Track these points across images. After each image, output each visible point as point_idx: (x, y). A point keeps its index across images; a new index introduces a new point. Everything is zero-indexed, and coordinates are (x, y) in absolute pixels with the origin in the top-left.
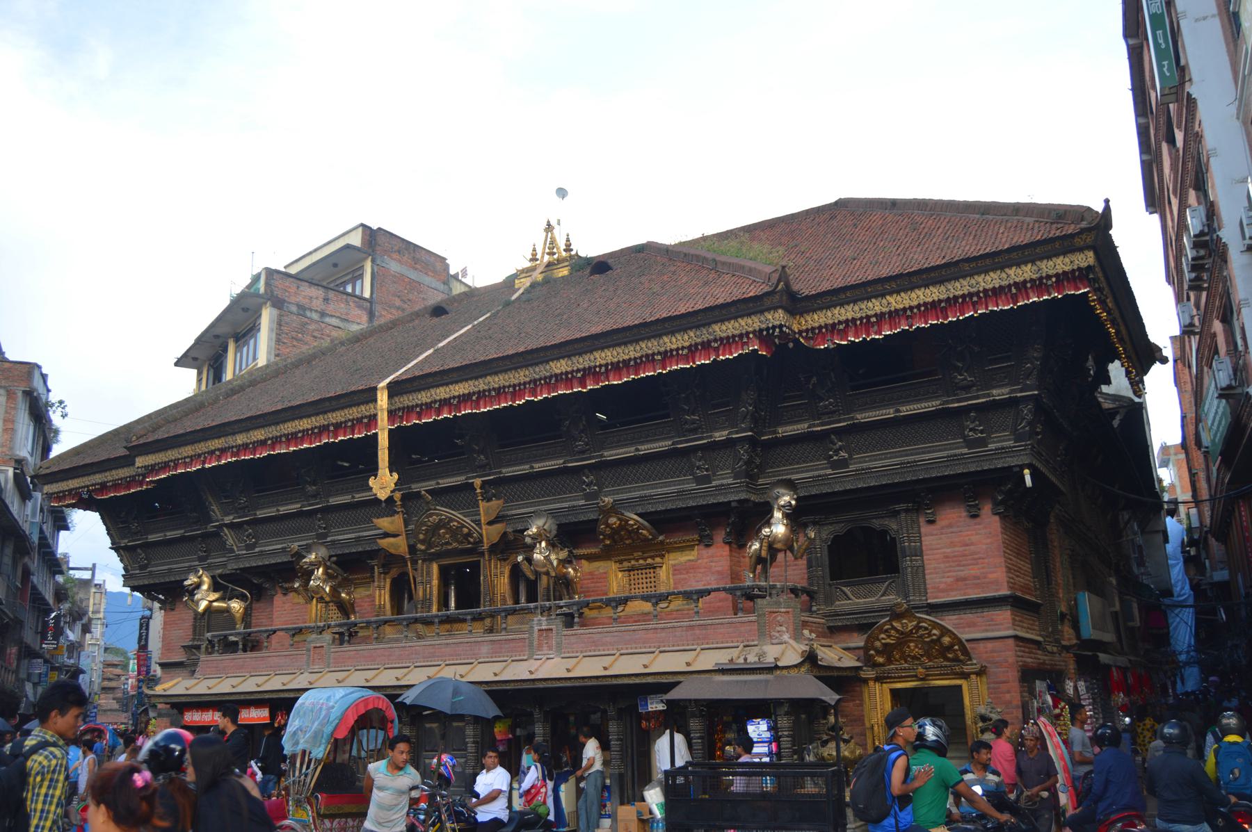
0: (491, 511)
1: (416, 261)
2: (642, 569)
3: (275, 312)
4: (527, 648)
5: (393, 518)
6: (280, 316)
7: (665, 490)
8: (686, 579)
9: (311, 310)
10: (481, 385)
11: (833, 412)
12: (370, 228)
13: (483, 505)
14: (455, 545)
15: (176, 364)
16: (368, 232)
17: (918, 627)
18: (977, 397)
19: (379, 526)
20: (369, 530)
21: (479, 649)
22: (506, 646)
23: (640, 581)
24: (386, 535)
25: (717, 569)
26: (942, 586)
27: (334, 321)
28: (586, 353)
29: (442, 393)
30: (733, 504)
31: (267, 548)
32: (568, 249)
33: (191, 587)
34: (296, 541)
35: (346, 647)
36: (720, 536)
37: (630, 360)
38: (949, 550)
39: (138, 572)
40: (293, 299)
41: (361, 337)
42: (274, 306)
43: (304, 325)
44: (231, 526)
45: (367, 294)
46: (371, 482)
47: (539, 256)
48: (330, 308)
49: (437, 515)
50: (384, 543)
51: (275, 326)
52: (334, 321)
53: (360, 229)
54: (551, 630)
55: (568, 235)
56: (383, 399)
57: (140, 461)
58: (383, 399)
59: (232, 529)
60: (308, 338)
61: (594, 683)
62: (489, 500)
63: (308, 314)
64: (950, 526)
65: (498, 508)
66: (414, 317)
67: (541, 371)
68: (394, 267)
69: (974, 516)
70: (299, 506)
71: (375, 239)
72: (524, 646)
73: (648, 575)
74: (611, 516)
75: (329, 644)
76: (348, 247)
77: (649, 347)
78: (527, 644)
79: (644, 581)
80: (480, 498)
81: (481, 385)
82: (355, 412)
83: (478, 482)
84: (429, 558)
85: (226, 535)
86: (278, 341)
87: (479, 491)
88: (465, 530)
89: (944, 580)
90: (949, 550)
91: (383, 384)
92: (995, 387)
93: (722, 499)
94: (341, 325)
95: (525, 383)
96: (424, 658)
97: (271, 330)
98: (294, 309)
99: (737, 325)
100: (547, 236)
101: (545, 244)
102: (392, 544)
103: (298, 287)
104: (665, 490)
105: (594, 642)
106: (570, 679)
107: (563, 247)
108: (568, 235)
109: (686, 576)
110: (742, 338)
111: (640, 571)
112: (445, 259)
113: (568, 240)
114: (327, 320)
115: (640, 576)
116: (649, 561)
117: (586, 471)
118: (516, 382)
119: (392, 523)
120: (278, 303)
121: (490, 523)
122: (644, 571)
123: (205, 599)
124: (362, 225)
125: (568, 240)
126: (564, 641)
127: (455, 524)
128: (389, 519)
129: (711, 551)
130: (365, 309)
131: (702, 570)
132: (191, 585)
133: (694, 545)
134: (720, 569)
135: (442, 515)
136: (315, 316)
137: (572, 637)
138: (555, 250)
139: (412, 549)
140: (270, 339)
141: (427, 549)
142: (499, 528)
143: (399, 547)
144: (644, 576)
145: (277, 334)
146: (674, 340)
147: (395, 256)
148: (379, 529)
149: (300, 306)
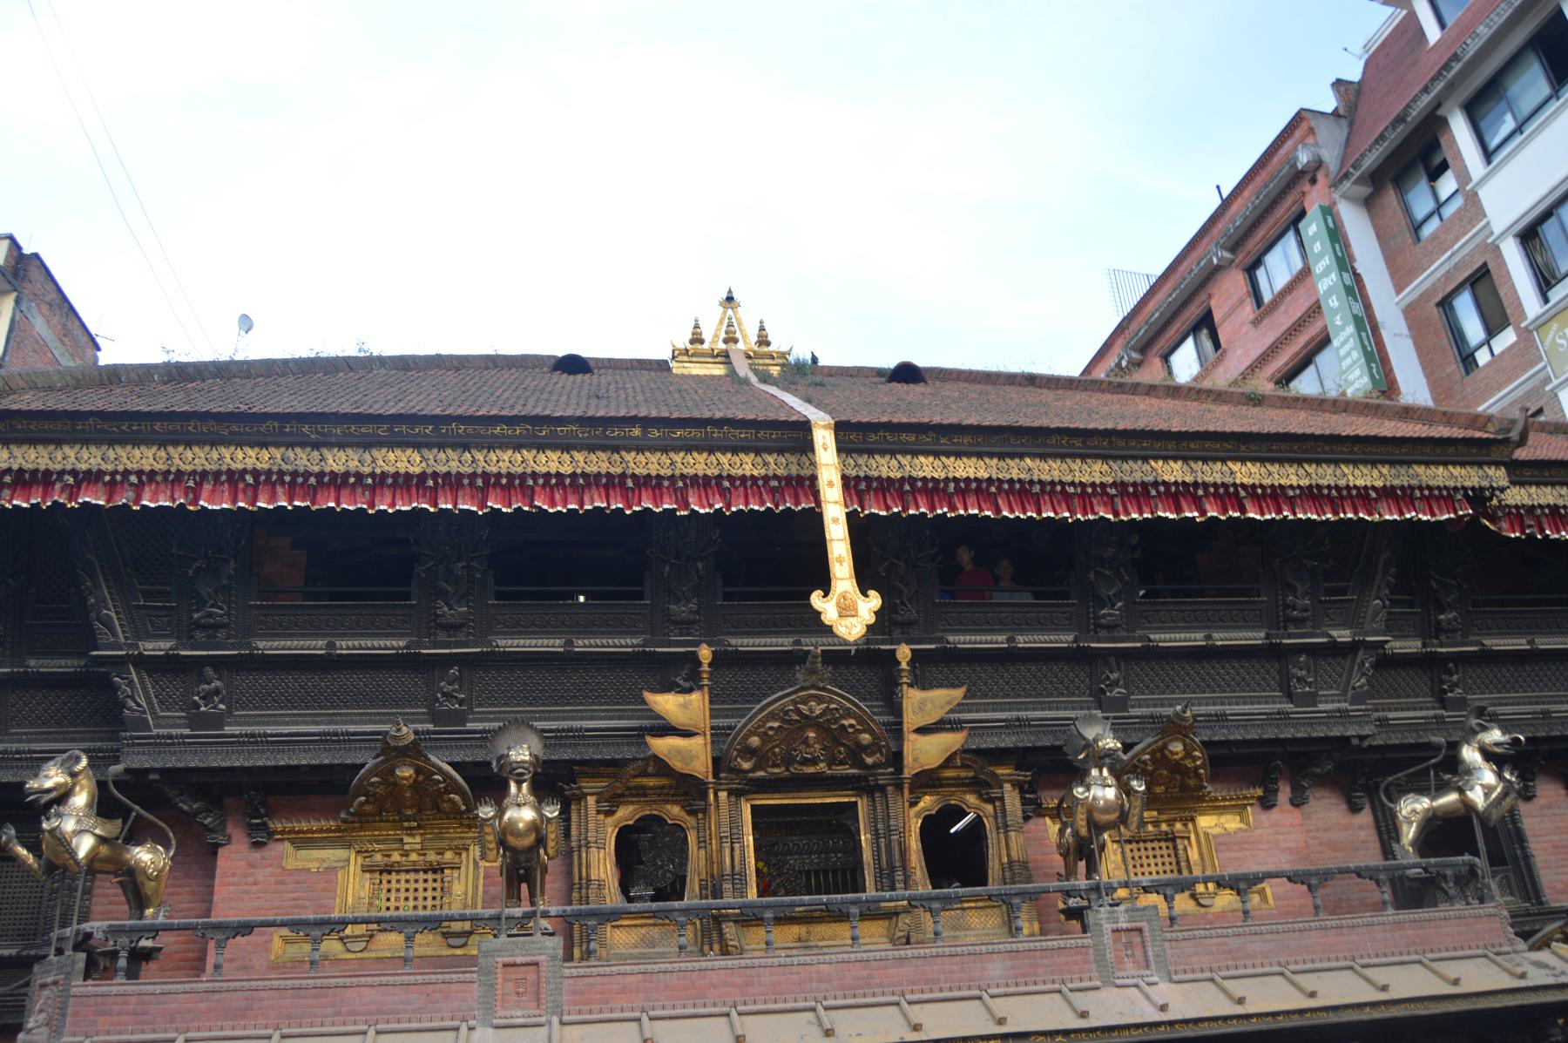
0: (929, 706)
1: (66, 333)
2: (1145, 841)
4: (1094, 966)
5: (687, 697)
7: (1247, 708)
8: (1239, 859)
10: (1015, 470)
11: (1454, 631)
12: (19, 248)
14: (822, 766)
19: (657, 708)
20: (592, 718)
21: (983, 969)
22: (1045, 961)
23: (1145, 861)
24: (666, 729)
25: (1288, 845)
28: (1215, 460)
30: (1355, 742)
31: (270, 730)
32: (763, 341)
33: (46, 798)
34: (413, 722)
36: (1284, 793)
37: (1291, 487)
38: (1556, 838)
41: (412, 365)
44: (143, 663)
46: (816, 599)
47: (707, 336)
49: (820, 700)
50: (662, 745)
53: (6, 243)
54: (1140, 930)
55: (761, 322)
59: (150, 672)
61: (1296, 1022)
62: (921, 683)
64: (1549, 806)
65: (949, 703)
66: (490, 365)
67: (1135, 472)
70: (402, 643)
72: (1086, 962)
73: (1158, 853)
74: (1176, 740)
75: (554, 958)
77: (1325, 475)
78: (1092, 957)
79: (1152, 861)
81: (1015, 470)
83: (904, 652)
84: (736, 794)
85: (131, 683)
87: (904, 665)
89: (1561, 877)
90: (1556, 838)
93: (1336, 732)
95: (1103, 485)
96: (843, 988)
99: (1446, 473)
100: (725, 313)
101: (721, 322)
102: (679, 751)
104: (1247, 708)
105: (1230, 952)
106: (1248, 1017)
107: (753, 338)
108: (761, 322)
109: (1240, 854)
110: (1445, 497)
111: (1142, 845)
112: (99, 349)
113: (762, 329)
115: (1143, 853)
116: (1164, 827)
117: (1112, 660)
119: (685, 706)
121: (922, 731)
122: (1149, 845)
124: (11, 238)
125: (762, 329)
126: (1169, 952)
127: (853, 722)
128: (681, 698)
129: (1274, 815)
132: (49, 791)
134: (1293, 845)
135: (831, 701)
137: (1184, 944)
138: (738, 335)
141: (752, 770)
143: (693, 758)
144: (1150, 853)
146: (1357, 472)
147: (45, 308)
148: (659, 717)
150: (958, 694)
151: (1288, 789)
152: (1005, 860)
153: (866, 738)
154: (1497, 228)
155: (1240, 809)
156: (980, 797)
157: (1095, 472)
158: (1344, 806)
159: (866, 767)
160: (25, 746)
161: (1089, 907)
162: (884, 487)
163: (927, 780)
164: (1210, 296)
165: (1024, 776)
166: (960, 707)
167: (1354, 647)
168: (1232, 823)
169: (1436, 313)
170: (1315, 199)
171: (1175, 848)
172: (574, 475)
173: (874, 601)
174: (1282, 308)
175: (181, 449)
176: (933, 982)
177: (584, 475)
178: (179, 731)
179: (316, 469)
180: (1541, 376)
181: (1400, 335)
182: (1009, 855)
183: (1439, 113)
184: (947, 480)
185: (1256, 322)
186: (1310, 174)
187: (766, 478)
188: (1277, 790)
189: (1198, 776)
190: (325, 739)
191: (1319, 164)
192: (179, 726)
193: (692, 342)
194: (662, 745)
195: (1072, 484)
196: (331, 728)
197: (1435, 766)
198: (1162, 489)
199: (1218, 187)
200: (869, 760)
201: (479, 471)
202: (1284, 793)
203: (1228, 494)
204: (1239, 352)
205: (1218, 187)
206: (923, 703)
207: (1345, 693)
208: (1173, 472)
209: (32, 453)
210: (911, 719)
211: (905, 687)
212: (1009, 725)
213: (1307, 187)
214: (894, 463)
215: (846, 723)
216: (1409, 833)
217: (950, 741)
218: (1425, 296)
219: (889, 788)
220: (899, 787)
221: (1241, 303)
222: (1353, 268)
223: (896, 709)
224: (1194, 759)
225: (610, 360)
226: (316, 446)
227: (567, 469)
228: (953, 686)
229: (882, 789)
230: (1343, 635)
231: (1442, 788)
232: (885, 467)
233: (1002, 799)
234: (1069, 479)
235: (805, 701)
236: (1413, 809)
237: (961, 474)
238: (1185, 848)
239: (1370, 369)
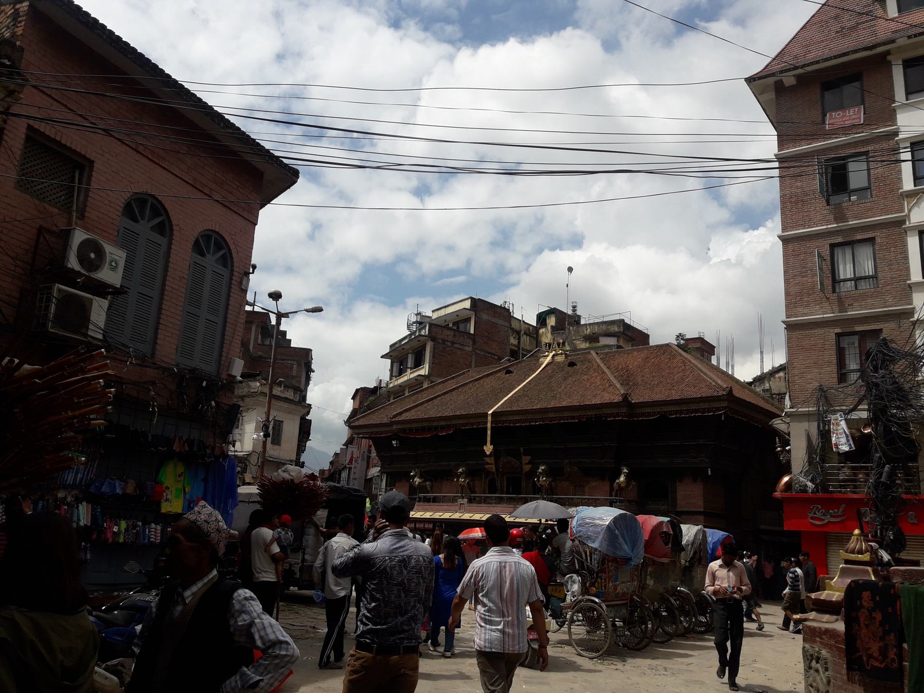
3: (432, 343)
6: (434, 345)
9: (448, 341)
13: (524, 458)
15: (381, 357)
16: (473, 301)
24: (488, 464)
27: (457, 346)
29: (511, 418)
35: (472, 505)
40: (440, 336)
42: (432, 340)
45: (472, 332)
46: (485, 448)
51: (432, 350)
52: (457, 346)
53: (470, 300)
56: (489, 418)
57: (394, 427)
58: (489, 418)
62: (525, 456)
63: (446, 343)
68: (485, 317)
76: (465, 309)
82: (479, 420)
83: (522, 450)
88: (517, 466)
91: (490, 412)
94: (461, 347)
97: (430, 352)
98: (440, 341)
103: (442, 331)
114: (455, 345)
116: (582, 484)
121: (526, 464)
124: (471, 298)
136: (449, 344)
139: (497, 470)
140: (430, 356)
145: (433, 354)
150: (530, 457)
194: (486, 466)
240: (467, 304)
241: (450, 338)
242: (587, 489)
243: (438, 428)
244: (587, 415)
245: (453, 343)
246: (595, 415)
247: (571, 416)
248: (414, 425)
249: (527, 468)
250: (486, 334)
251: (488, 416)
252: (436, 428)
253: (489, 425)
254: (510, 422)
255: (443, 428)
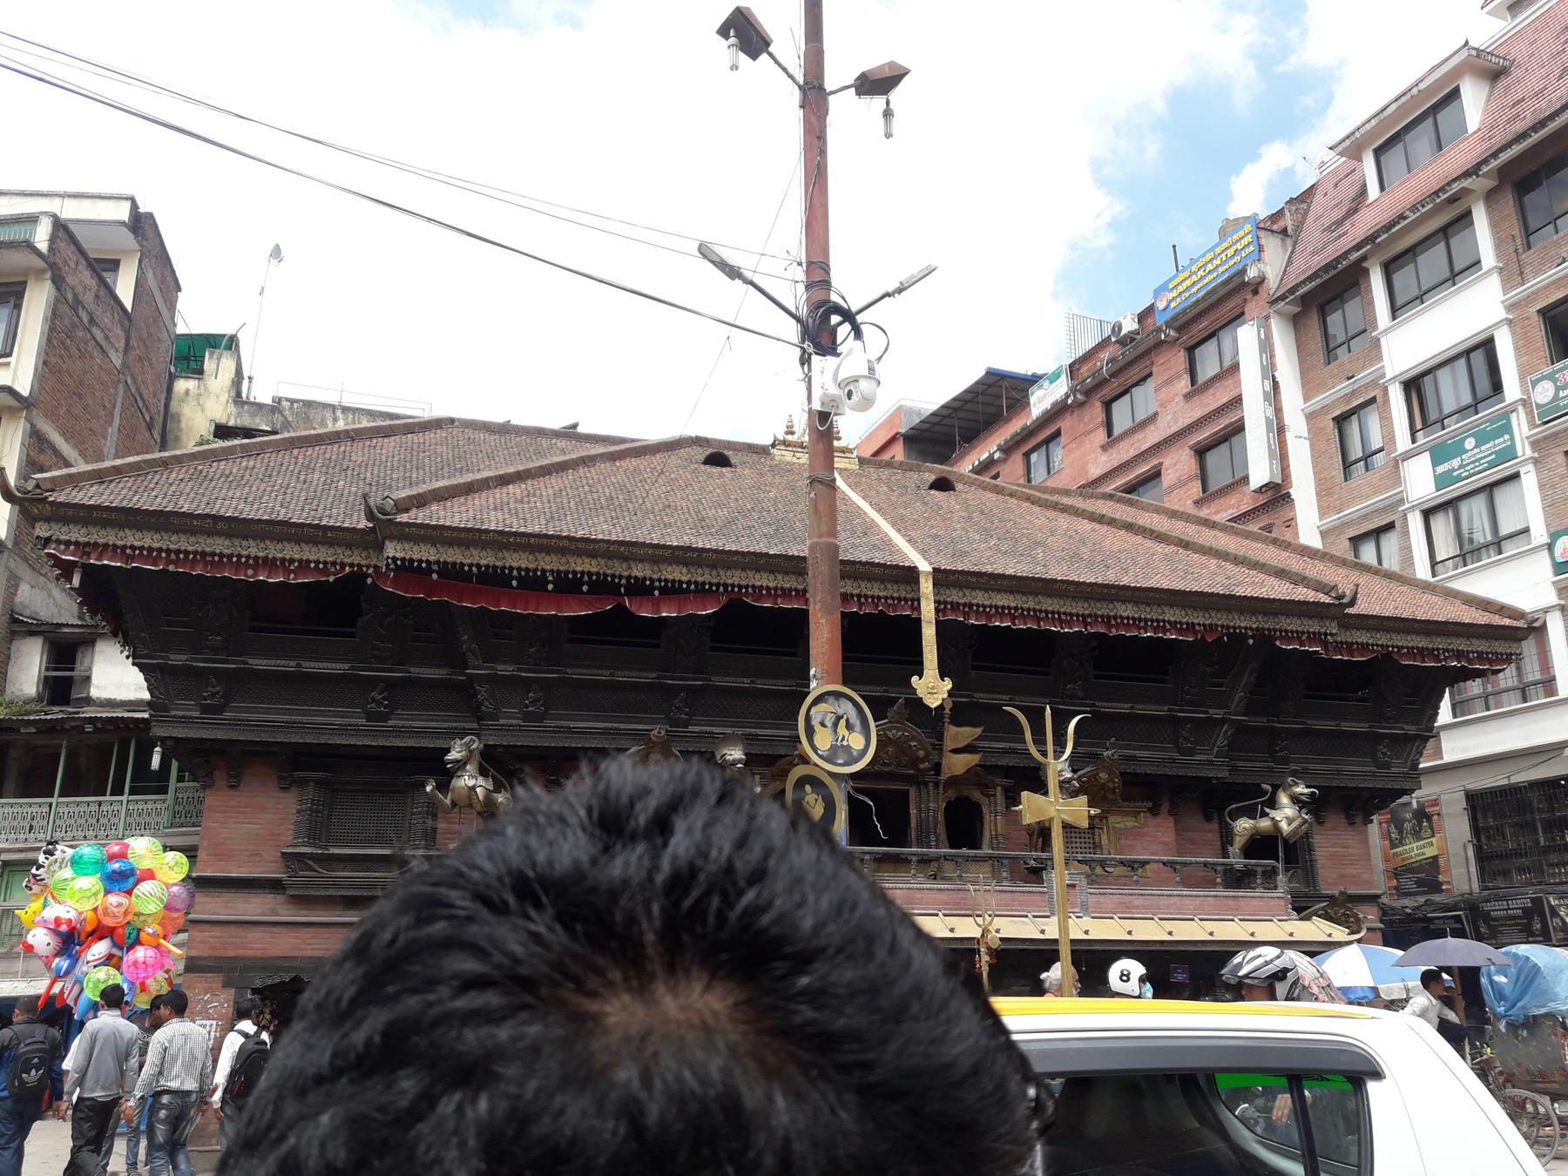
0: (960, 737)
3: (53, 290)
6: (57, 300)
10: (1030, 603)
17: (1344, 914)
18: (1394, 728)
23: (1074, 840)
25: (1164, 839)
26: (1330, 881)
29: (979, 598)
36: (1165, 808)
37: (1199, 624)
39: (197, 714)
42: (54, 281)
43: (74, 326)
48: (98, 312)
49: (898, 729)
53: (127, 205)
56: (926, 586)
57: (393, 550)
58: (926, 586)
60: (74, 350)
67: (1103, 609)
68: (151, 281)
69: (1351, 824)
70: (654, 675)
71: (142, 225)
79: (1078, 840)
80: (947, 720)
86: (49, 340)
92: (1406, 723)
94: (104, 344)
98: (70, 297)
109: (1133, 842)
112: (179, 289)
114: (94, 330)
118: (1074, 611)
120: (58, 281)
121: (955, 751)
123: (469, 781)
124: (133, 200)
129: (1158, 820)
130: (125, 331)
131: (1149, 839)
133: (1139, 812)
142: (972, 759)
149: (75, 296)
150: (978, 731)
151: (1168, 804)
152: (994, 833)
153: (921, 753)
154: (1389, 375)
155: (1136, 814)
156: (982, 793)
157: (1079, 608)
158: (1201, 817)
159: (920, 770)
160: (408, 723)
161: (1045, 869)
162: (955, 606)
163: (954, 781)
164: (1152, 363)
165: (1008, 782)
166: (980, 738)
167: (1222, 721)
168: (1130, 823)
169: (1330, 426)
170: (1254, 307)
171: (1093, 834)
172: (776, 589)
173: (948, 684)
174: (1211, 391)
175: (543, 554)
176: (959, 904)
177: (782, 589)
178: (514, 722)
179: (626, 574)
180: (1398, 497)
181: (1301, 437)
182: (996, 831)
183: (1364, 265)
184: (991, 606)
185: (1188, 397)
186: (1257, 286)
187: (886, 598)
188: (1161, 805)
189: (1114, 792)
190: (606, 732)
191: (1262, 280)
192: (515, 718)
193: (787, 433)
195: (1065, 613)
196: (610, 725)
197: (1261, 802)
198: (1119, 620)
199: (1174, 247)
200: (922, 766)
201: (722, 582)
202: (1165, 808)
203: (1159, 625)
204: (1169, 417)
205: (1174, 247)
206: (957, 734)
207: (1212, 749)
208: (1126, 610)
209: (450, 551)
210: (949, 744)
211: (946, 724)
212: (1004, 752)
213: (1249, 296)
214: (961, 594)
215: (913, 744)
216: (1239, 842)
217: (972, 759)
218: (1325, 409)
219: (931, 784)
220: (937, 785)
221: (1179, 377)
222: (1273, 376)
223: (940, 737)
224: (1114, 782)
225: (729, 442)
226: (626, 559)
227: (771, 585)
228: (975, 726)
229: (926, 784)
230: (1217, 714)
231: (1265, 815)
232: (955, 596)
233: (995, 795)
234: (1062, 610)
235: (890, 729)
236: (1243, 825)
237: (1000, 603)
238: (1100, 835)
239: (1271, 464)
240: (122, 212)
241: (88, 298)
242: (1104, 841)
243: (652, 588)
244: (1234, 628)
245: (92, 321)
246: (1257, 629)
247: (1187, 623)
248: (518, 561)
249: (957, 764)
250: (145, 336)
251: (922, 580)
252: (639, 588)
253: (928, 610)
254: (981, 611)
255: (672, 590)
